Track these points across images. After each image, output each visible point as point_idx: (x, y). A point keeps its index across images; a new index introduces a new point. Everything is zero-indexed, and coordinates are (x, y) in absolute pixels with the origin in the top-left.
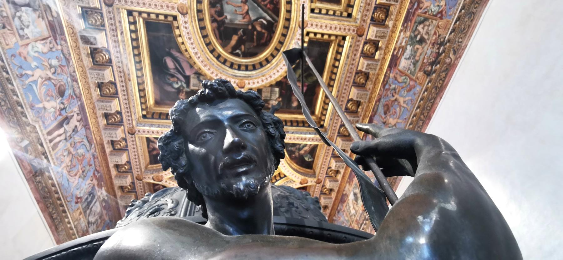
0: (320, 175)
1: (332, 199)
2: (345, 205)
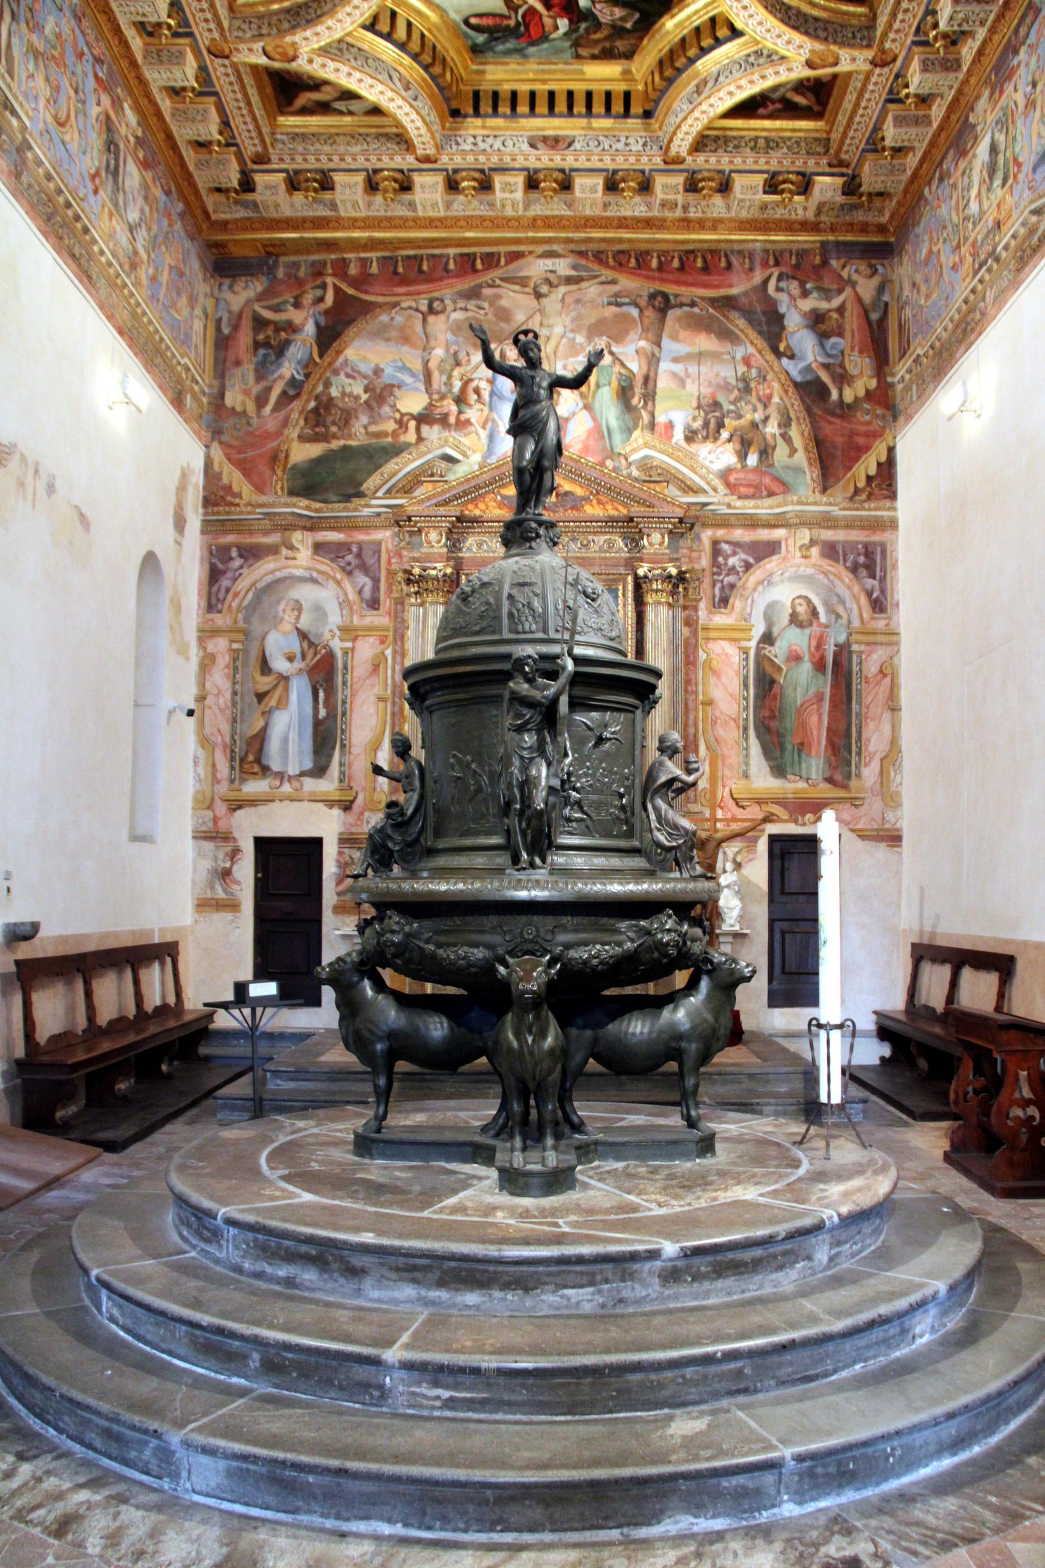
0: (892, 36)
1: (930, 123)
2: (962, 165)
